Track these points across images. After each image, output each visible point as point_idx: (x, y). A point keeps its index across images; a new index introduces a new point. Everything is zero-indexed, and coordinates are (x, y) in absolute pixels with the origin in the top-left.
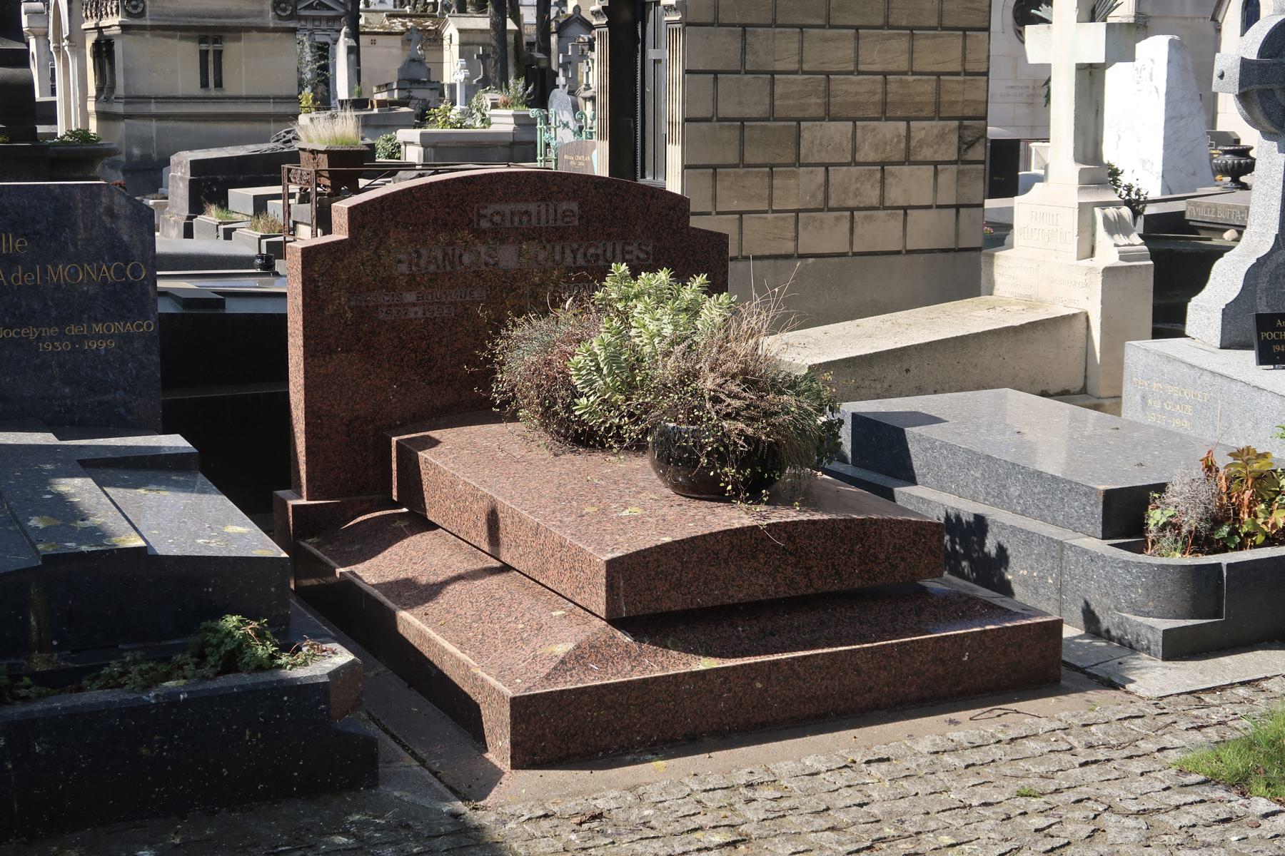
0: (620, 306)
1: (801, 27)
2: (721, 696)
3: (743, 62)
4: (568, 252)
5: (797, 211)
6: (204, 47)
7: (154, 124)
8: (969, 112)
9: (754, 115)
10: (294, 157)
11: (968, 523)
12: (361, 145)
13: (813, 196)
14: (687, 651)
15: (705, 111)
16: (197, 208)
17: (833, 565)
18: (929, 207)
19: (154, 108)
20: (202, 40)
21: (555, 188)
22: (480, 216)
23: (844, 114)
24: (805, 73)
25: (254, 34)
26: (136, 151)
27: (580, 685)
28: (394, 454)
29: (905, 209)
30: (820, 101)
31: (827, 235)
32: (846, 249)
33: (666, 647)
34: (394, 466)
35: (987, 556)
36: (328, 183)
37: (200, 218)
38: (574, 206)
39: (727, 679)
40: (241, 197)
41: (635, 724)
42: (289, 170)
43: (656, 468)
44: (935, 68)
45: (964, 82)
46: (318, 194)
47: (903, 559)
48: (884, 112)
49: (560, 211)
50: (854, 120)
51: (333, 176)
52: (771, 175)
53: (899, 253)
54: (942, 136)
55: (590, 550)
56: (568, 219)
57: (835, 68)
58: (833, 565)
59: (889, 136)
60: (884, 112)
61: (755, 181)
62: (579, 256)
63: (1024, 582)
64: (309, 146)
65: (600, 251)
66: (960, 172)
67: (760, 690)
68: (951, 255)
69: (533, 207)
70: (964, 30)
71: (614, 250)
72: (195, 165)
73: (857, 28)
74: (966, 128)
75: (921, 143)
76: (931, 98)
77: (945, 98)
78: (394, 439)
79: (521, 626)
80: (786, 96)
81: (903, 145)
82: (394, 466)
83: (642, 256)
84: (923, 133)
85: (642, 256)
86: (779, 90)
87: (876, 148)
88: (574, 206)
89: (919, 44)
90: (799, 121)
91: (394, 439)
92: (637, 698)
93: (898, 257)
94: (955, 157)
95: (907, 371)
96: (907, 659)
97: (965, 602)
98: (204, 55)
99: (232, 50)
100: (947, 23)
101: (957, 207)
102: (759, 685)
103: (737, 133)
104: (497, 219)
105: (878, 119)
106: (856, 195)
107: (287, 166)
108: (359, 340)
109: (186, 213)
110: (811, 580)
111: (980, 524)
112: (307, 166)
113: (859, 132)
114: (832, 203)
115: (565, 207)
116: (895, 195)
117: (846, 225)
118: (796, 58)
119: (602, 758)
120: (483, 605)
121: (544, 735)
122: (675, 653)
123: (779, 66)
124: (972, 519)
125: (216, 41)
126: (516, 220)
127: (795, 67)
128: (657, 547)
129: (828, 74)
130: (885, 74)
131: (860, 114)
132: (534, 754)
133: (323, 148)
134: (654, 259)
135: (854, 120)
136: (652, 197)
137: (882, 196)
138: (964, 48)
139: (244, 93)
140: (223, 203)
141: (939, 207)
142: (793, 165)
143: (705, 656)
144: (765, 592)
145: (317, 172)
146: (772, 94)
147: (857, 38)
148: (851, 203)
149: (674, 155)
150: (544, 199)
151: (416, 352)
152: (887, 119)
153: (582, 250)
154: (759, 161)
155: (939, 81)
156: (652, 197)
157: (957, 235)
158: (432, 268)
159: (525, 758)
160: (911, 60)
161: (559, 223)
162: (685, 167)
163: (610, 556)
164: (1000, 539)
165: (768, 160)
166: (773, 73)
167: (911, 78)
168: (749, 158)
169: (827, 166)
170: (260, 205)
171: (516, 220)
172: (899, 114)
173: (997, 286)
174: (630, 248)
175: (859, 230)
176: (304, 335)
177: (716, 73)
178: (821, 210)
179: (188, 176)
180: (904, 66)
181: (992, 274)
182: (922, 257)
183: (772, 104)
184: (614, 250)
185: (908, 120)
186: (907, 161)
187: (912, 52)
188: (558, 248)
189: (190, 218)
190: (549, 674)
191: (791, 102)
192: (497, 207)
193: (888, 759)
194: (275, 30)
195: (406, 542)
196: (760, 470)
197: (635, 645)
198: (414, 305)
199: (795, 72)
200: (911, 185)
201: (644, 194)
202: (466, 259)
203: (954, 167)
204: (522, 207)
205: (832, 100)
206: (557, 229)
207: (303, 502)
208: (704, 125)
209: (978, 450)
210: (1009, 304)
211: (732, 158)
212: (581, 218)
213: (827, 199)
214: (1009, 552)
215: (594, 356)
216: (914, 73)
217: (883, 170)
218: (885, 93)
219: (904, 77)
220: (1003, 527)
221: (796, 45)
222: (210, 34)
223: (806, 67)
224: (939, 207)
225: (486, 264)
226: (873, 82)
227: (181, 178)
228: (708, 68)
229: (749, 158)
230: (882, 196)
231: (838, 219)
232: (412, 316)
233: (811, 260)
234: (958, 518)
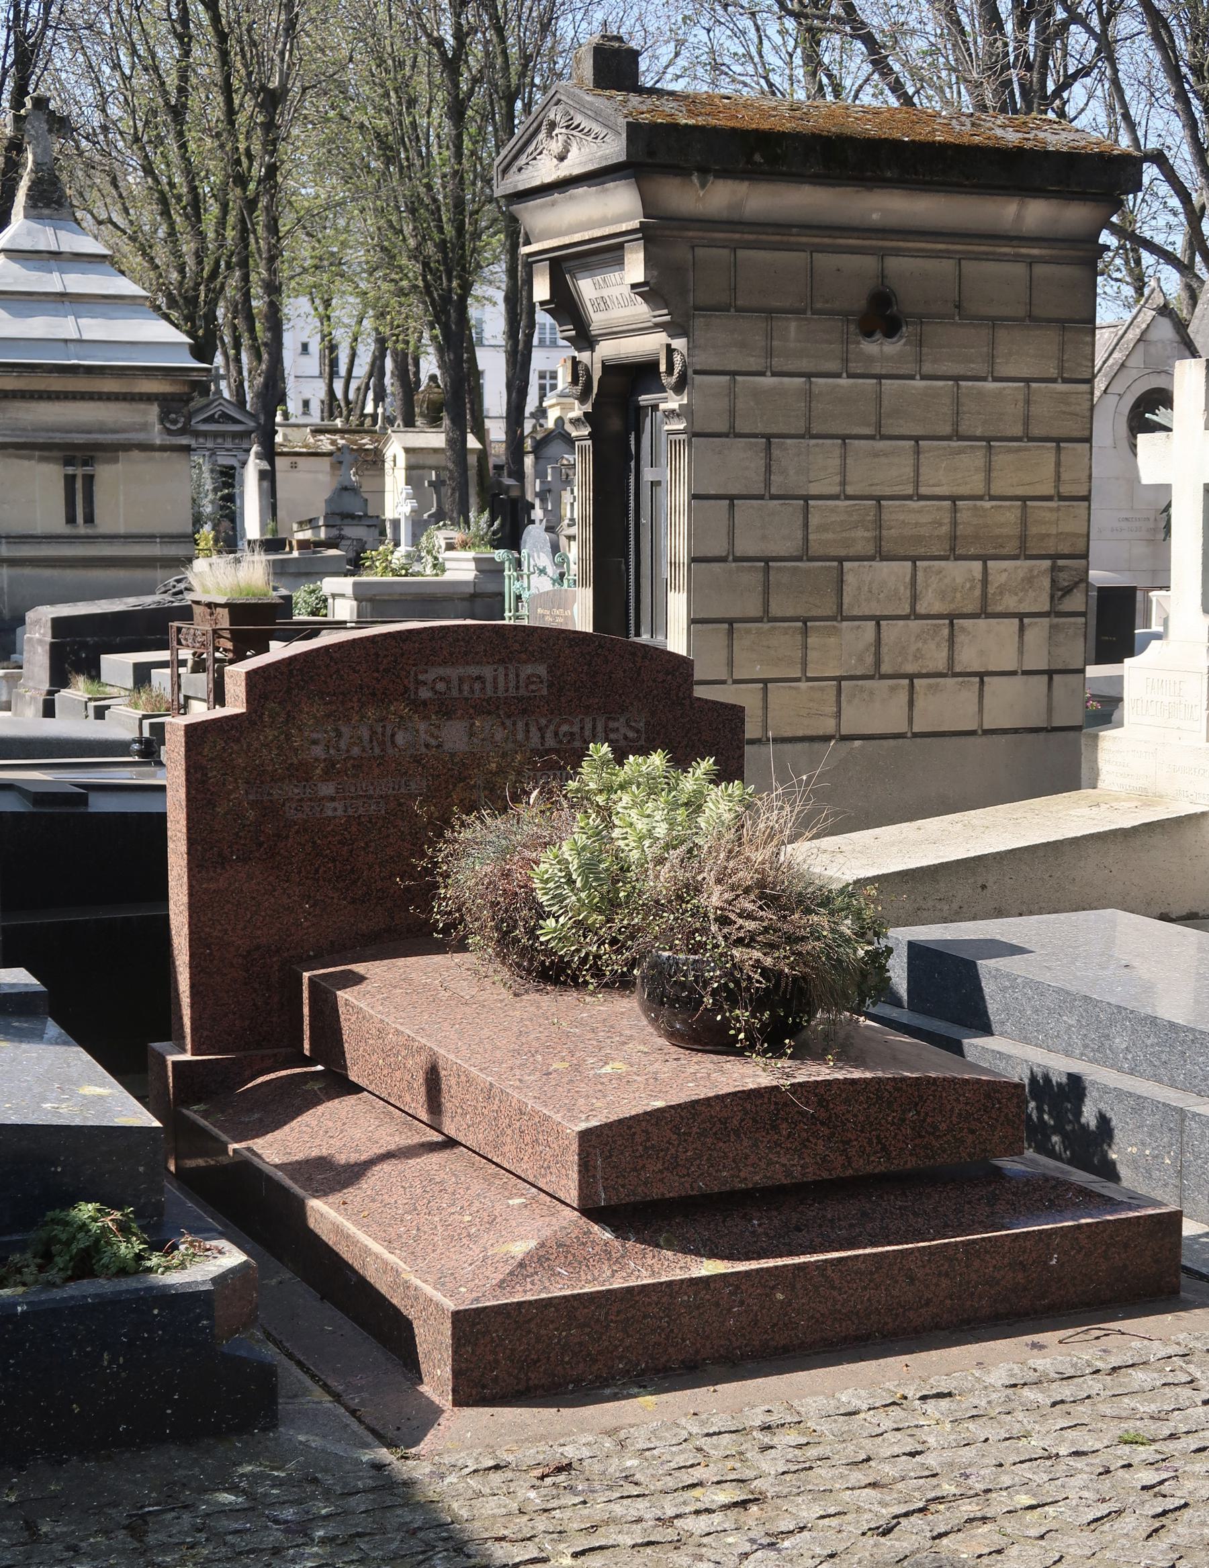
0: (600, 799)
1: (844, 438)
2: (729, 1310)
3: (768, 483)
4: (533, 729)
5: (839, 679)
6: (70, 470)
8: (1065, 549)
9: (782, 554)
10: (186, 613)
11: (1059, 1085)
12: (273, 596)
13: (861, 659)
14: (686, 1251)
15: (719, 549)
16: (59, 679)
17: (878, 1137)
18: (1013, 673)
20: (68, 462)
21: (517, 647)
22: (419, 683)
23: (902, 552)
24: (848, 498)
25: (136, 453)
27: (543, 1296)
28: (306, 994)
29: (981, 675)
30: (867, 534)
31: (878, 710)
32: (904, 728)
33: (657, 1246)
34: (306, 1010)
35: (1085, 1128)
36: (229, 645)
37: (64, 692)
38: (542, 670)
39: (738, 1287)
40: (117, 666)
41: (617, 1347)
42: (179, 630)
43: (646, 1011)
44: (1020, 491)
45: (1058, 509)
46: (216, 660)
47: (972, 1132)
48: (953, 549)
49: (523, 676)
50: (914, 560)
51: (236, 636)
52: (805, 632)
53: (972, 733)
54: (1029, 580)
55: (557, 1118)
56: (533, 687)
57: (888, 491)
58: (878, 1137)
59: (959, 580)
60: (953, 549)
61: (784, 641)
62: (549, 735)
63: (1134, 1162)
64: (206, 599)
65: (576, 729)
66: (1053, 628)
67: (782, 1302)
68: (1042, 735)
69: (487, 672)
70: (1058, 441)
71: (594, 728)
72: (59, 625)
73: (917, 439)
74: (1061, 569)
75: (1002, 590)
76: (1015, 531)
77: (1033, 530)
78: (306, 975)
79: (468, 1218)
80: (823, 528)
81: (978, 592)
82: (306, 1010)
83: (631, 734)
84: (1004, 576)
85: (631, 734)
86: (814, 520)
87: (942, 595)
88: (542, 670)
89: (999, 460)
90: (841, 560)
91: (306, 975)
92: (619, 1312)
93: (971, 739)
94: (1047, 608)
95: (984, 887)
96: (977, 1263)
97: (1054, 1187)
98: (70, 481)
99: (106, 474)
100: (1036, 431)
101: (1050, 673)
102: (780, 1296)
103: (760, 576)
104: (441, 686)
105: (945, 558)
106: (916, 658)
107: (176, 624)
108: (260, 845)
109: (46, 686)
110: (849, 1159)
111: (1075, 1086)
112: (202, 624)
113: (920, 574)
114: (886, 668)
115: (529, 671)
116: (968, 658)
117: (903, 697)
118: (837, 479)
119: (572, 1392)
120: (419, 1191)
121: (497, 1361)
122: (670, 1253)
123: (814, 489)
124: (1064, 1080)
125: (86, 463)
126: (466, 687)
127: (835, 490)
128: (646, 1113)
129: (879, 499)
130: (954, 499)
131: (922, 551)
132: (484, 1387)
133: (222, 600)
134: (647, 739)
135: (914, 560)
136: (644, 657)
137: (951, 659)
138: (1058, 464)
139: (122, 530)
140: (94, 673)
141: (1025, 673)
142: (833, 619)
143: (709, 1258)
144: (788, 1174)
145: (215, 631)
146: (806, 525)
147: (917, 452)
148: (910, 668)
149: (677, 606)
150: (502, 661)
151: (334, 860)
152: (958, 558)
153: (552, 727)
154: (790, 613)
155: (1025, 507)
157: (1050, 710)
158: (356, 751)
159: (473, 1390)
160: (988, 481)
161: (522, 692)
162: (692, 621)
163: (583, 1126)
164: (1102, 1105)
165: (800, 611)
166: (806, 498)
167: (988, 504)
168: (775, 611)
169: (878, 620)
170: (142, 674)
171: (466, 687)
172: (972, 551)
173: (1102, 777)
174: (616, 725)
175: (920, 703)
176: (189, 839)
177: (731, 498)
178: (871, 677)
179: (49, 639)
180: (979, 489)
181: (1096, 761)
182: (1003, 739)
183: (806, 539)
184: (594, 728)
185: (985, 559)
186: (984, 612)
187: (989, 470)
188: (520, 725)
189: (51, 693)
190: (503, 1281)
191: (830, 536)
192: (441, 671)
193: (950, 1395)
194: (163, 448)
195: (320, 1109)
196: (782, 1012)
197: (617, 1243)
198: (333, 799)
199: (835, 497)
200: (988, 643)
201: (634, 654)
202: (400, 739)
203: (1045, 621)
204: (474, 671)
205: (884, 533)
206: (520, 699)
207: (187, 1057)
208: (716, 566)
209: (1073, 989)
210: (1117, 799)
211: (754, 610)
213: (878, 662)
214: (1113, 1123)
215: (563, 862)
216: (992, 498)
217: (952, 624)
218: (954, 524)
219: (979, 503)
220: (1105, 1090)
221: (837, 462)
222: (78, 454)
223: (850, 490)
224: (1025, 673)
225: (427, 746)
226: (939, 509)
227: (40, 641)
228: (721, 492)
229: (775, 611)
230: (951, 659)
231: (893, 689)
232: (330, 813)
233: (857, 743)
234: (1047, 1078)
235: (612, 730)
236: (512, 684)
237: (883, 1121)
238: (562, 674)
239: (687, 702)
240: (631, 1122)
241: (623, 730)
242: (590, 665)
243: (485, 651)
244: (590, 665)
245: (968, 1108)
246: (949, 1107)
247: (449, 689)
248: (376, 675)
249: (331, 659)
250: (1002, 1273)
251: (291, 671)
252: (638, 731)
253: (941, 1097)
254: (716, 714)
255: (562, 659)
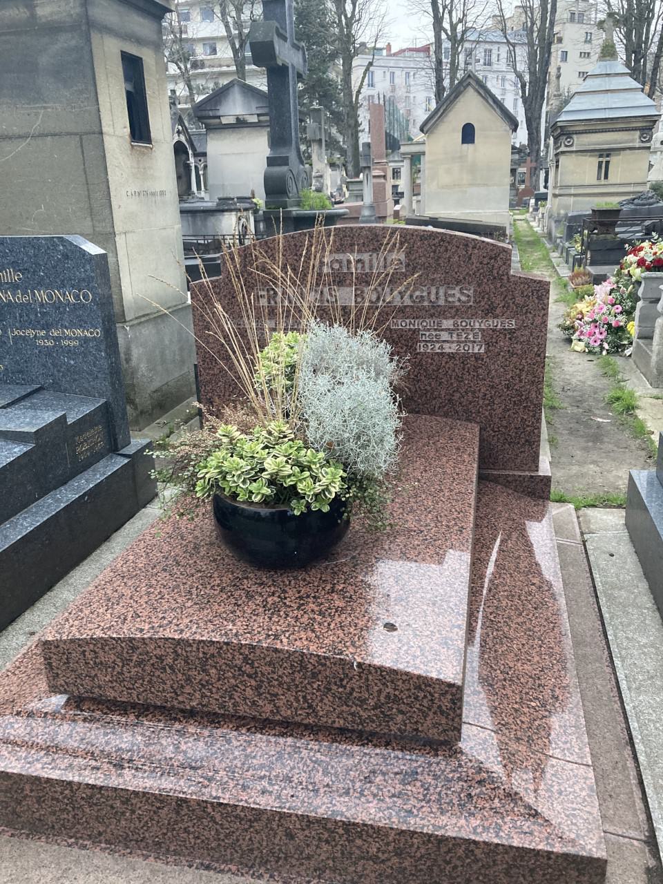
6: (601, 159)
7: (572, 199)
19: (572, 191)
20: (601, 156)
25: (628, 151)
26: (562, 212)
58: (304, 697)
65: (425, 294)
71: (437, 293)
83: (464, 298)
85: (464, 298)
125: (608, 156)
134: (475, 301)
136: (474, 248)
139: (618, 182)
153: (409, 292)
156: (474, 248)
184: (437, 293)
201: (467, 245)
212: (408, 265)
222: (605, 153)
235: (450, 295)
236: (382, 264)
237: (308, 687)
238: (415, 259)
239: (505, 278)
240: (80, 642)
241: (458, 295)
242: (435, 252)
243: (364, 243)
244: (435, 252)
245: (397, 693)
246: (376, 688)
247: (341, 267)
248: (295, 257)
249: (269, 248)
250: (386, 855)
251: (245, 255)
252: (468, 296)
253: (367, 680)
254: (527, 286)
255: (415, 248)
